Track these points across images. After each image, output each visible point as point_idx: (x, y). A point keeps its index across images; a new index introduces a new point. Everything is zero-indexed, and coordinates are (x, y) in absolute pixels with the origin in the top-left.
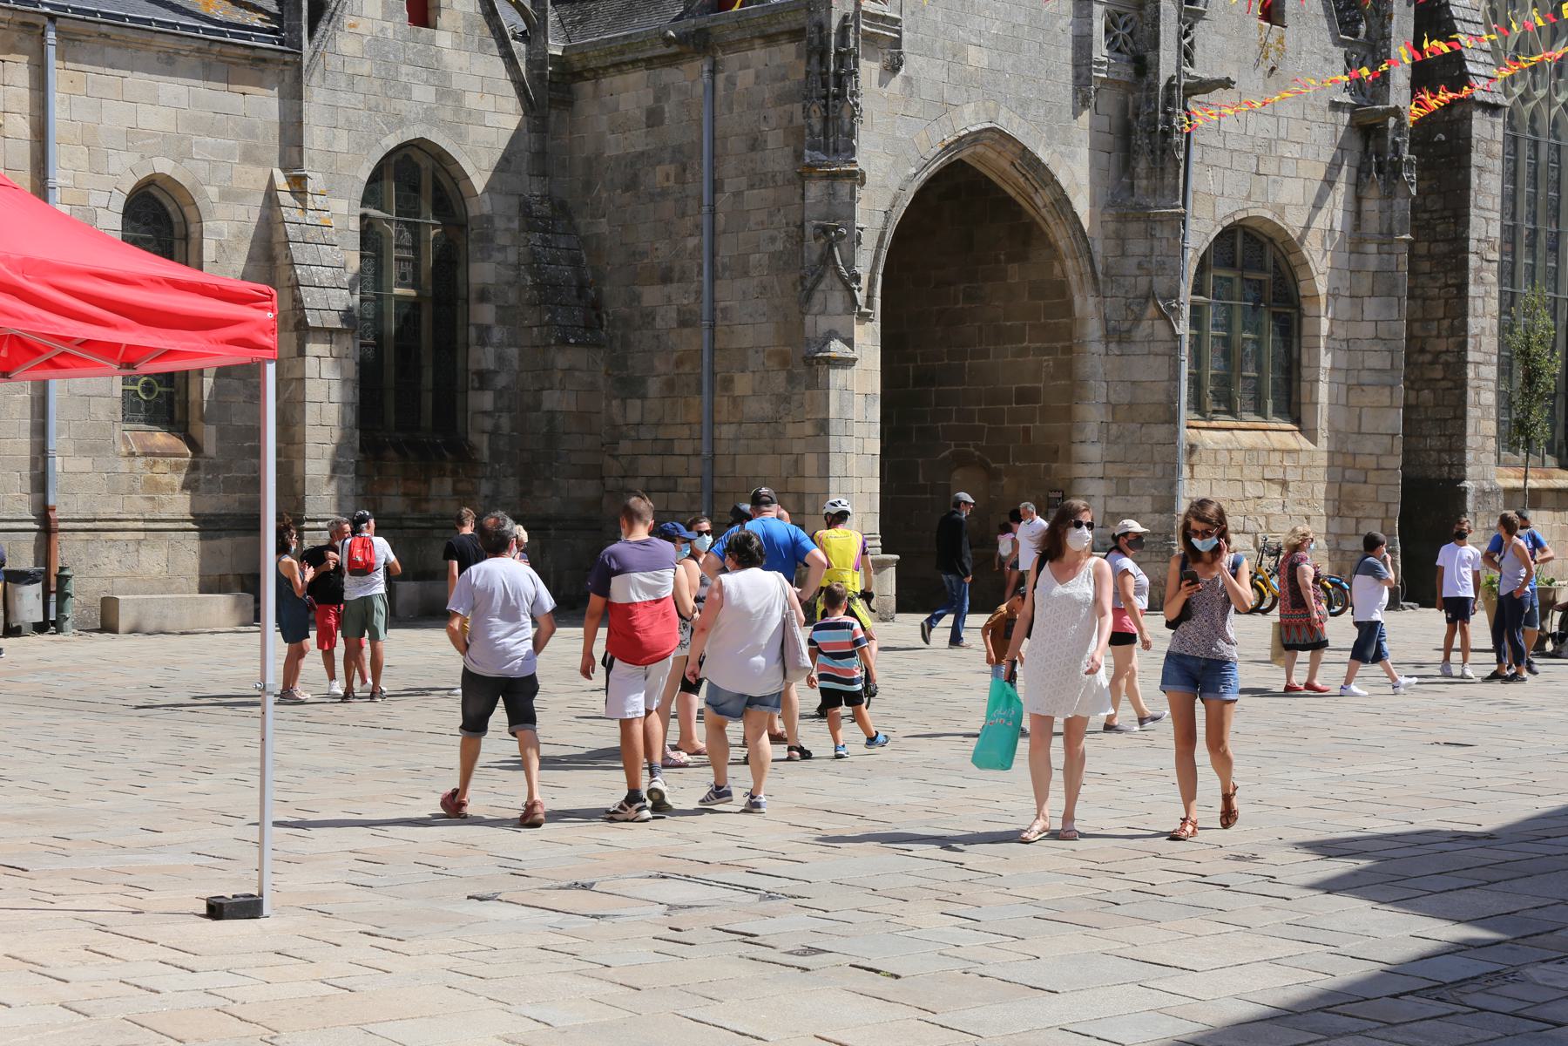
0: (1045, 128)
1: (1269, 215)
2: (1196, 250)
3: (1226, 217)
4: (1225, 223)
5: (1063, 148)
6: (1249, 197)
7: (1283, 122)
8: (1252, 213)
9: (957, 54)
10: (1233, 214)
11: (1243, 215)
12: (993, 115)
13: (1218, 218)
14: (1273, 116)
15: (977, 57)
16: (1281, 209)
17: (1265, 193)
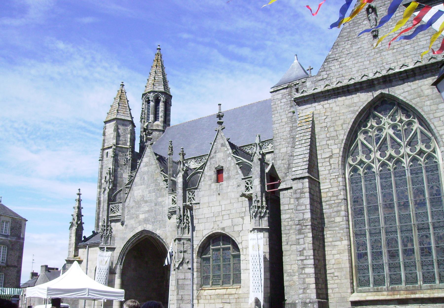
0: (159, 226)
1: (220, 231)
2: (198, 245)
3: (206, 235)
4: (206, 236)
5: (163, 229)
6: (213, 228)
7: (223, 206)
8: (214, 232)
9: (137, 217)
10: (209, 233)
11: (212, 233)
12: (145, 227)
13: (204, 235)
14: (220, 205)
15: (142, 216)
16: (223, 229)
17: (218, 226)
